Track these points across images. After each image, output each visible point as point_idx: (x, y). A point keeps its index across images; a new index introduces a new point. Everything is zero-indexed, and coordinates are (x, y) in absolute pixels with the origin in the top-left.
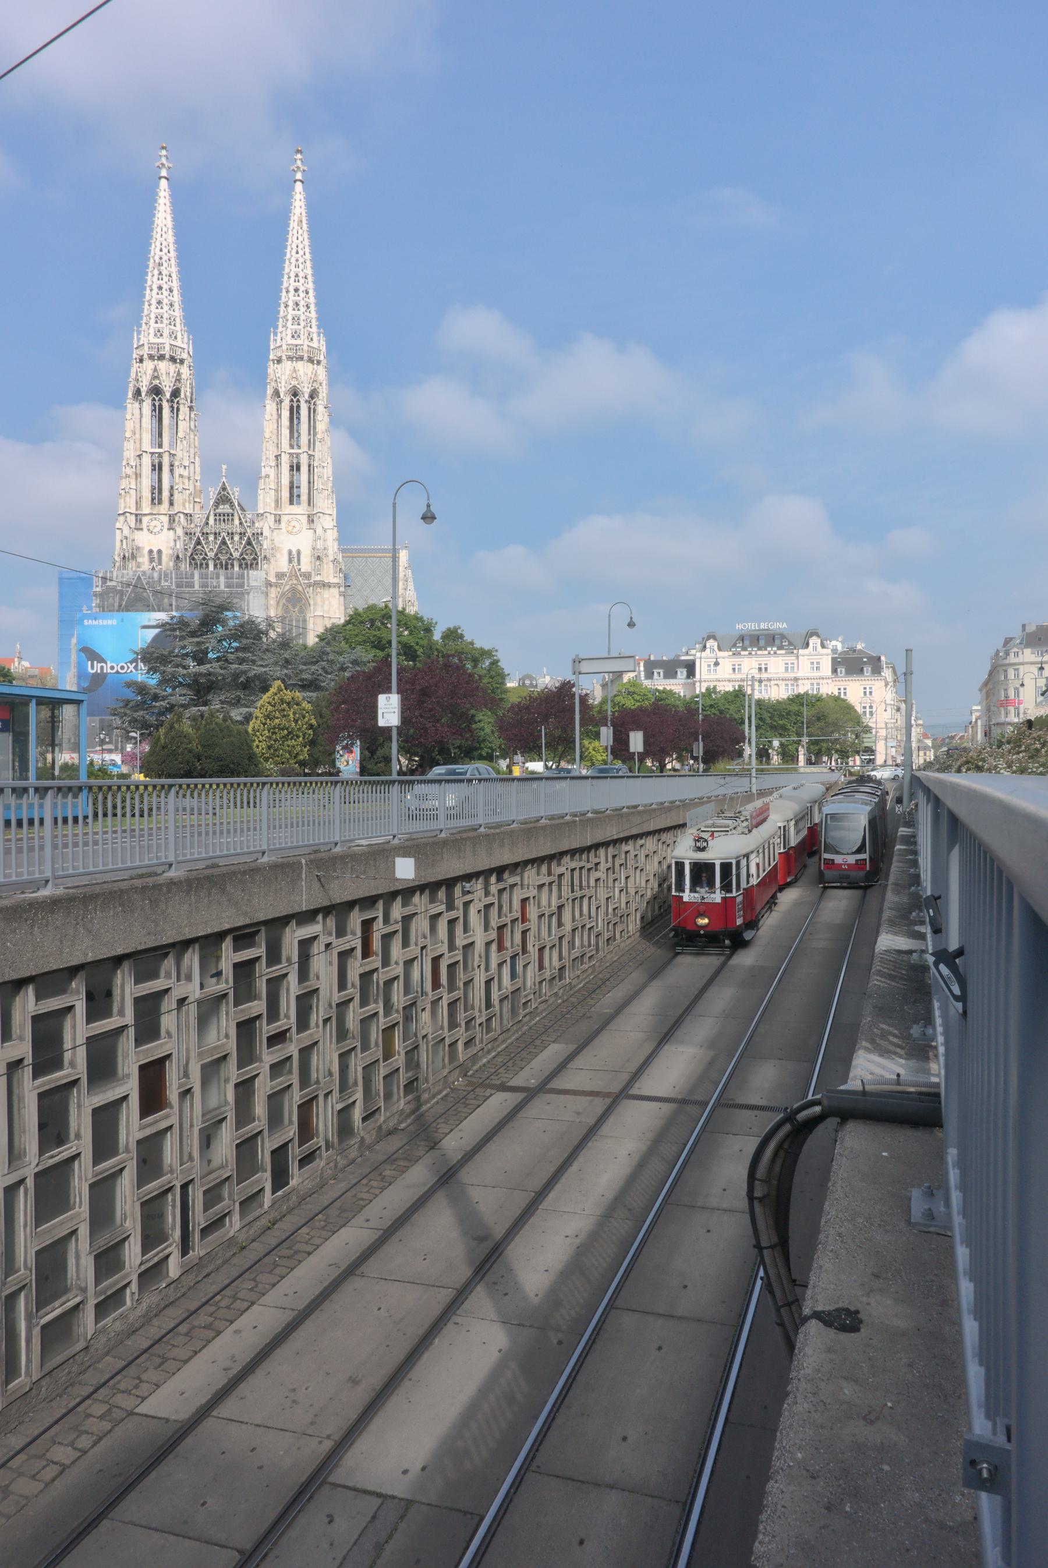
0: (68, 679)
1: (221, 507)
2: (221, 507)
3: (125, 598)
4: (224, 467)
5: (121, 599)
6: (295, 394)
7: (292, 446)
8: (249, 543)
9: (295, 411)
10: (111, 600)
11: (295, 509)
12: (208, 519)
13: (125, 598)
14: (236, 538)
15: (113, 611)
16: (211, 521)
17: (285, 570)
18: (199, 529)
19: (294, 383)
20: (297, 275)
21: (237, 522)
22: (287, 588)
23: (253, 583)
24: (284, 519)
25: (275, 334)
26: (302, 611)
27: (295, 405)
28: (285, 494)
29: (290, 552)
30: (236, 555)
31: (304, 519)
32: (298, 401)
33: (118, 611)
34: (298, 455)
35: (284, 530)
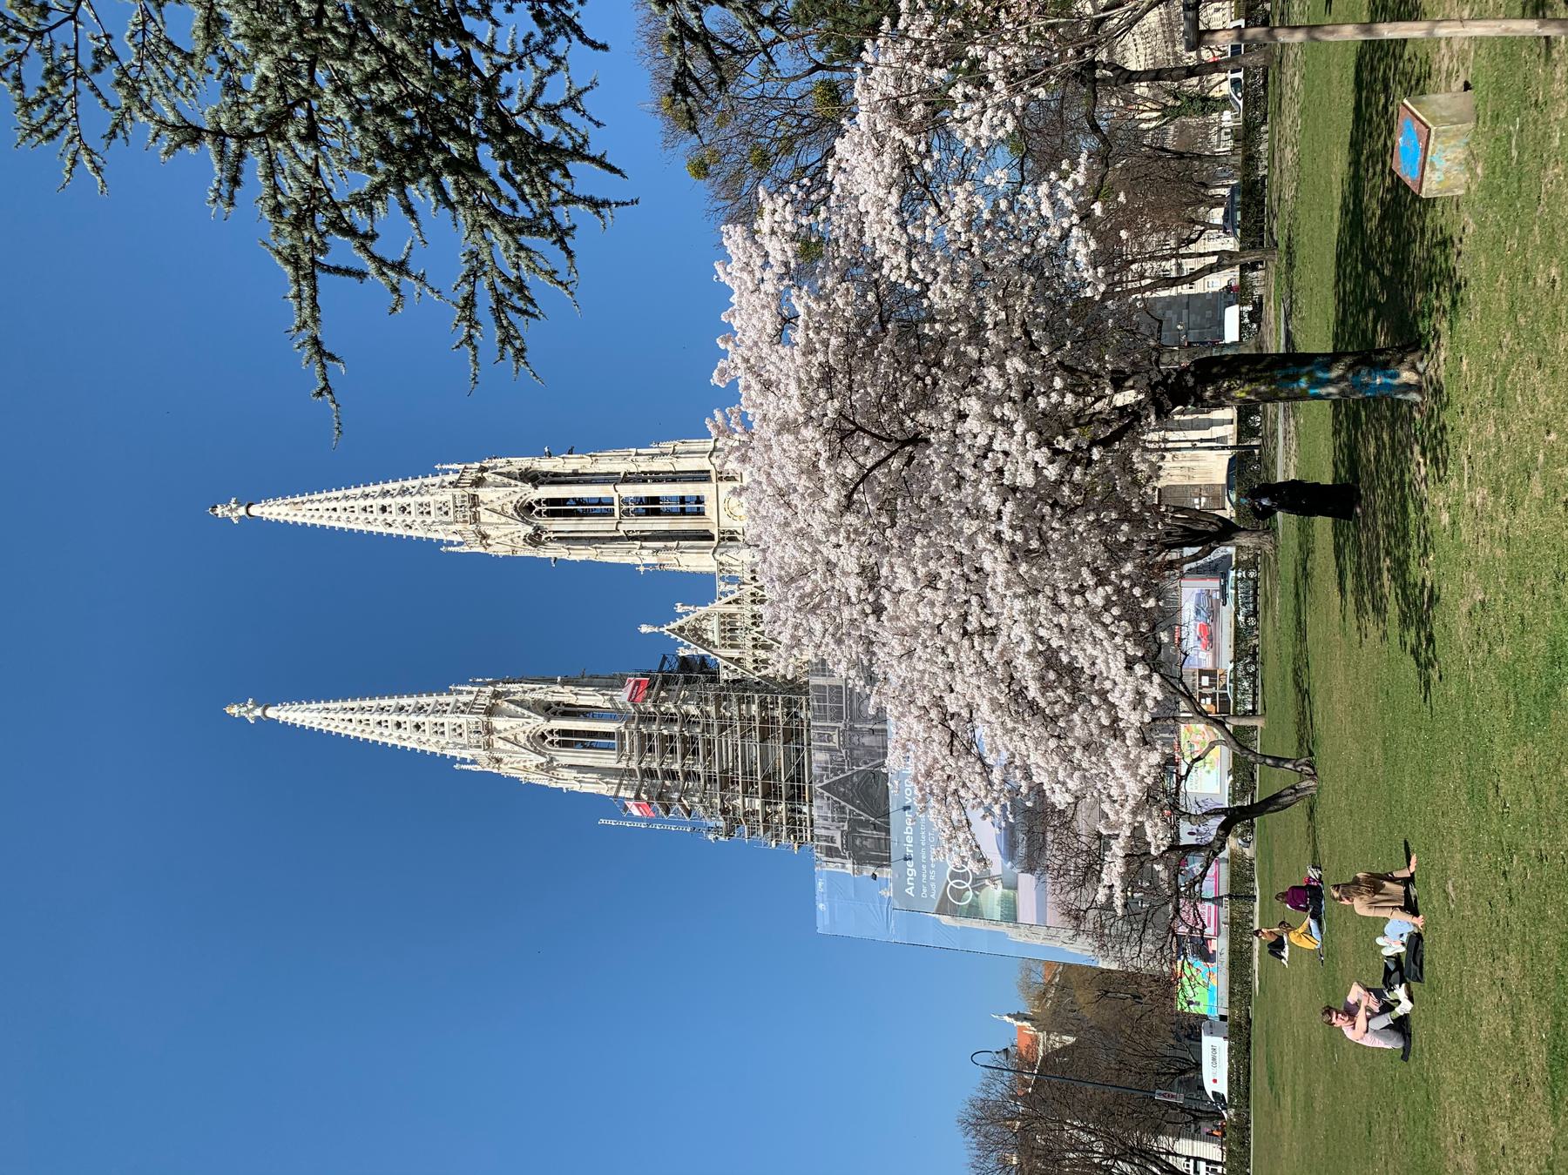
0: (1022, 940)
2: (710, 636)
3: (864, 817)
4: (645, 629)
5: (865, 824)
6: (530, 507)
7: (611, 513)
9: (558, 508)
10: (867, 843)
11: (709, 507)
12: (730, 659)
13: (864, 817)
15: (887, 841)
16: (735, 654)
19: (510, 510)
20: (365, 509)
21: (733, 609)
24: (727, 524)
25: (451, 543)
28: (686, 524)
32: (538, 502)
33: (888, 831)
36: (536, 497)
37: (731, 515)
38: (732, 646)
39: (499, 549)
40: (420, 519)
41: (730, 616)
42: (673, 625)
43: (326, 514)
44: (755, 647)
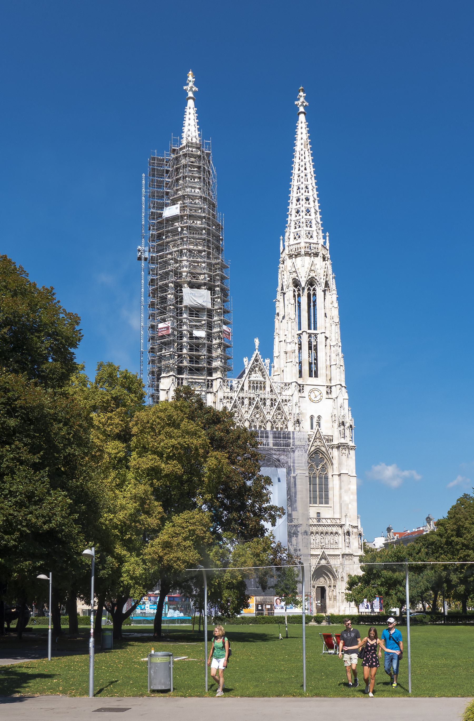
1: (255, 375)
4: (257, 341)
7: (309, 328)
8: (279, 409)
11: (313, 380)
12: (243, 385)
14: (268, 403)
16: (246, 388)
17: (310, 433)
18: (236, 394)
19: (312, 274)
21: (268, 389)
22: (313, 448)
23: (297, 443)
24: (307, 389)
26: (324, 468)
27: (312, 293)
29: (312, 417)
30: (269, 417)
31: (324, 390)
32: (314, 290)
34: (316, 335)
35: (307, 398)
36: (317, 288)
37: (311, 391)
38: (250, 386)
39: (289, 262)
40: (303, 220)
41: (265, 387)
42: (260, 356)
43: (302, 163)
44: (250, 398)
